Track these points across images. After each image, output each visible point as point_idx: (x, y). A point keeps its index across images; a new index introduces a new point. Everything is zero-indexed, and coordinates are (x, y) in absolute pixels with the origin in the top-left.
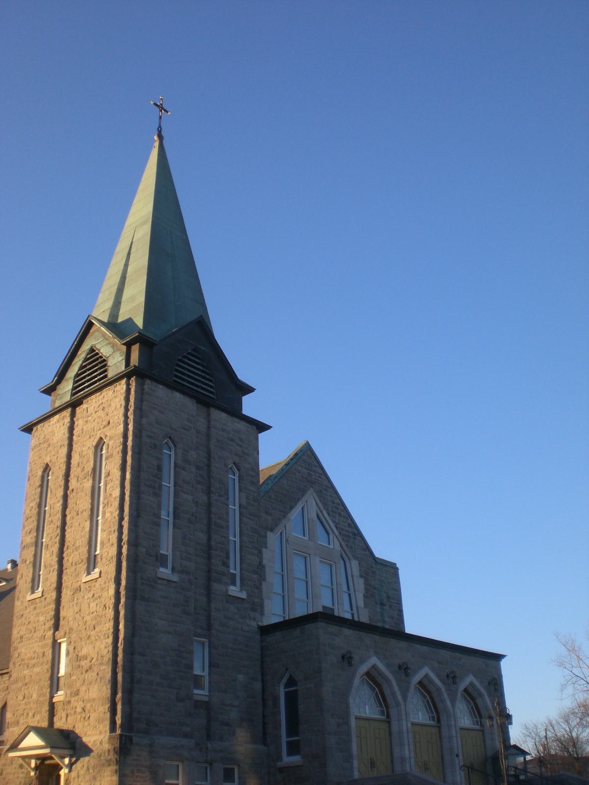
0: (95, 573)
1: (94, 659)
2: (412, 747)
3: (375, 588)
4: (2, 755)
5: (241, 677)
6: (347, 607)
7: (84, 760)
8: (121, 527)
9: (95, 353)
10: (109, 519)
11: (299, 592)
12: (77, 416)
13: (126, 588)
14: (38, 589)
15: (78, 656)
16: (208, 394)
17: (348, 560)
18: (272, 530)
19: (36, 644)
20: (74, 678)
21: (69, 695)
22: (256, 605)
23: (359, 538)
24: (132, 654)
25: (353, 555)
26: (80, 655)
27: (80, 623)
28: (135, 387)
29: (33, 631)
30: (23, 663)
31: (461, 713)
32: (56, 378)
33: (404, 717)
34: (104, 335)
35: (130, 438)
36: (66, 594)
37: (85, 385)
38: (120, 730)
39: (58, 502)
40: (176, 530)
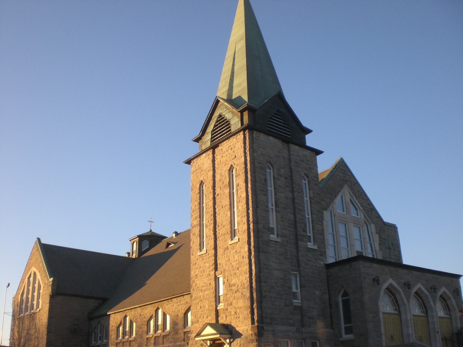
0: (236, 239)
1: (240, 285)
2: (413, 329)
3: (385, 240)
4: (190, 340)
5: (317, 292)
6: (369, 251)
7: (238, 341)
8: (248, 214)
9: (222, 117)
10: (241, 210)
11: (343, 243)
12: (216, 154)
13: (254, 247)
14: (203, 249)
15: (230, 284)
16: (287, 136)
17: (369, 224)
18: (326, 210)
19: (205, 279)
20: (228, 296)
21: (227, 306)
22: (323, 253)
23: (374, 211)
24: (260, 282)
25: (371, 221)
26: (231, 283)
27: (230, 266)
28: (249, 136)
29: (203, 272)
30: (198, 289)
31: (439, 309)
32: (201, 133)
33: (408, 312)
34: (226, 107)
35: (249, 165)
36: (220, 251)
37: (218, 136)
38: (257, 323)
39: (210, 201)
40: (278, 213)
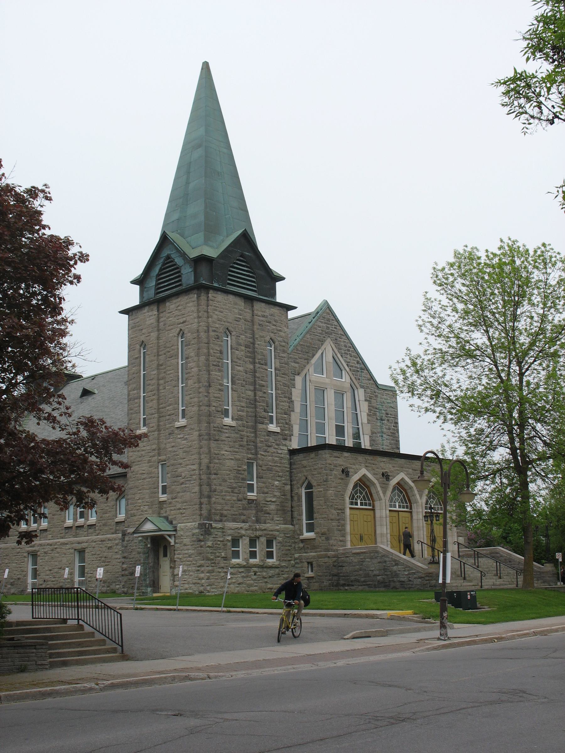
22: (286, 436)
23: (365, 371)
